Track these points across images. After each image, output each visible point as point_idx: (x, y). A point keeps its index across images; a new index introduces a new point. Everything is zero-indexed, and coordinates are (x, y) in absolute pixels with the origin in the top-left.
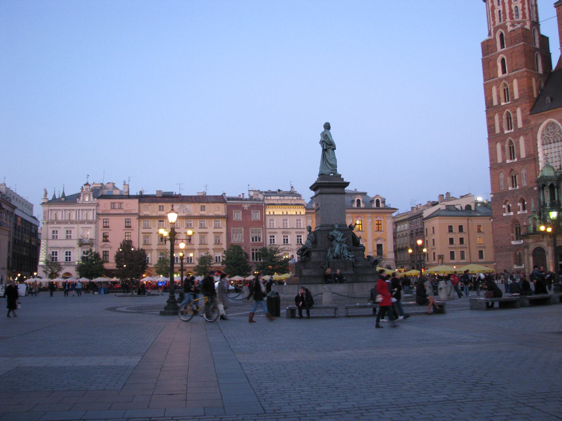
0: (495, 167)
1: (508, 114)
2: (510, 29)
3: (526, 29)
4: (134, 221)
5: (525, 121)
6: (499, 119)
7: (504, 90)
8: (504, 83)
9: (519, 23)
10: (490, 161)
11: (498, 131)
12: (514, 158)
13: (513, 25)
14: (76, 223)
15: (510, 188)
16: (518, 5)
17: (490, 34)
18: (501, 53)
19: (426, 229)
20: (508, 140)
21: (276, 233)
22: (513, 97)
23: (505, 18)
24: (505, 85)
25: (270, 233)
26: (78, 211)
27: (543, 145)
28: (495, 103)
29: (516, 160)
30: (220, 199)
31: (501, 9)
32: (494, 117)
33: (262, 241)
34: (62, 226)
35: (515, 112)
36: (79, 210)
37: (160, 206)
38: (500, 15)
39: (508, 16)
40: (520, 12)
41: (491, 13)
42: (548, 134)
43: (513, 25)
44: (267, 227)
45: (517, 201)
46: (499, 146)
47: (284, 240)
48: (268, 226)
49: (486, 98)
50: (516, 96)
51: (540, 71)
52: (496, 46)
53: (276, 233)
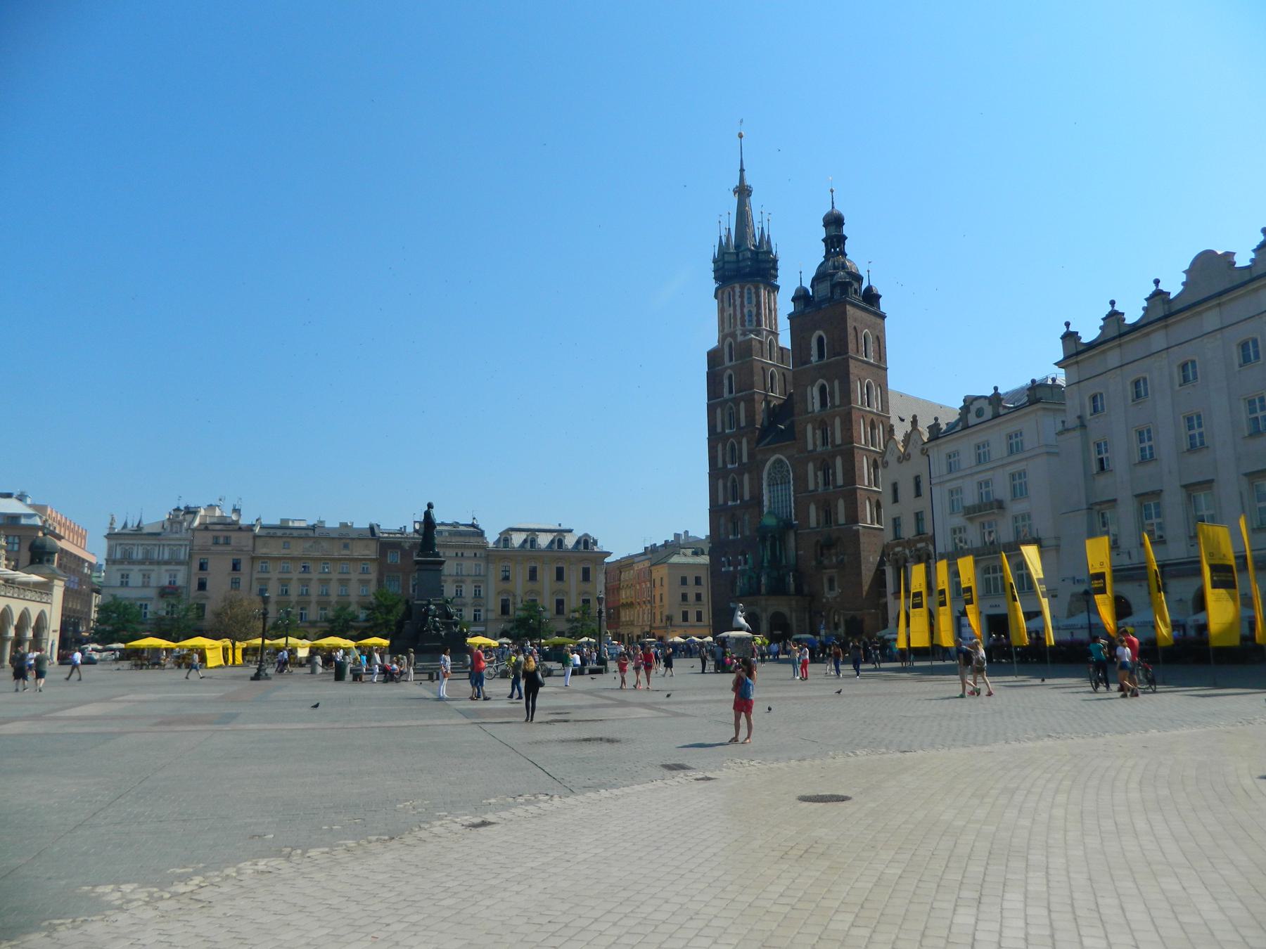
0: (716, 511)
1: (733, 446)
2: (740, 338)
4: (244, 567)
5: (751, 456)
6: (723, 450)
7: (730, 414)
9: (751, 332)
11: (720, 464)
13: (744, 334)
14: (159, 563)
16: (752, 309)
18: (729, 367)
19: (654, 580)
20: (730, 477)
23: (735, 325)
24: (731, 408)
26: (161, 548)
27: (769, 485)
28: (719, 429)
29: (739, 501)
31: (732, 312)
34: (136, 568)
35: (740, 443)
36: (164, 545)
37: (284, 543)
39: (739, 322)
40: (754, 319)
42: (774, 473)
46: (720, 483)
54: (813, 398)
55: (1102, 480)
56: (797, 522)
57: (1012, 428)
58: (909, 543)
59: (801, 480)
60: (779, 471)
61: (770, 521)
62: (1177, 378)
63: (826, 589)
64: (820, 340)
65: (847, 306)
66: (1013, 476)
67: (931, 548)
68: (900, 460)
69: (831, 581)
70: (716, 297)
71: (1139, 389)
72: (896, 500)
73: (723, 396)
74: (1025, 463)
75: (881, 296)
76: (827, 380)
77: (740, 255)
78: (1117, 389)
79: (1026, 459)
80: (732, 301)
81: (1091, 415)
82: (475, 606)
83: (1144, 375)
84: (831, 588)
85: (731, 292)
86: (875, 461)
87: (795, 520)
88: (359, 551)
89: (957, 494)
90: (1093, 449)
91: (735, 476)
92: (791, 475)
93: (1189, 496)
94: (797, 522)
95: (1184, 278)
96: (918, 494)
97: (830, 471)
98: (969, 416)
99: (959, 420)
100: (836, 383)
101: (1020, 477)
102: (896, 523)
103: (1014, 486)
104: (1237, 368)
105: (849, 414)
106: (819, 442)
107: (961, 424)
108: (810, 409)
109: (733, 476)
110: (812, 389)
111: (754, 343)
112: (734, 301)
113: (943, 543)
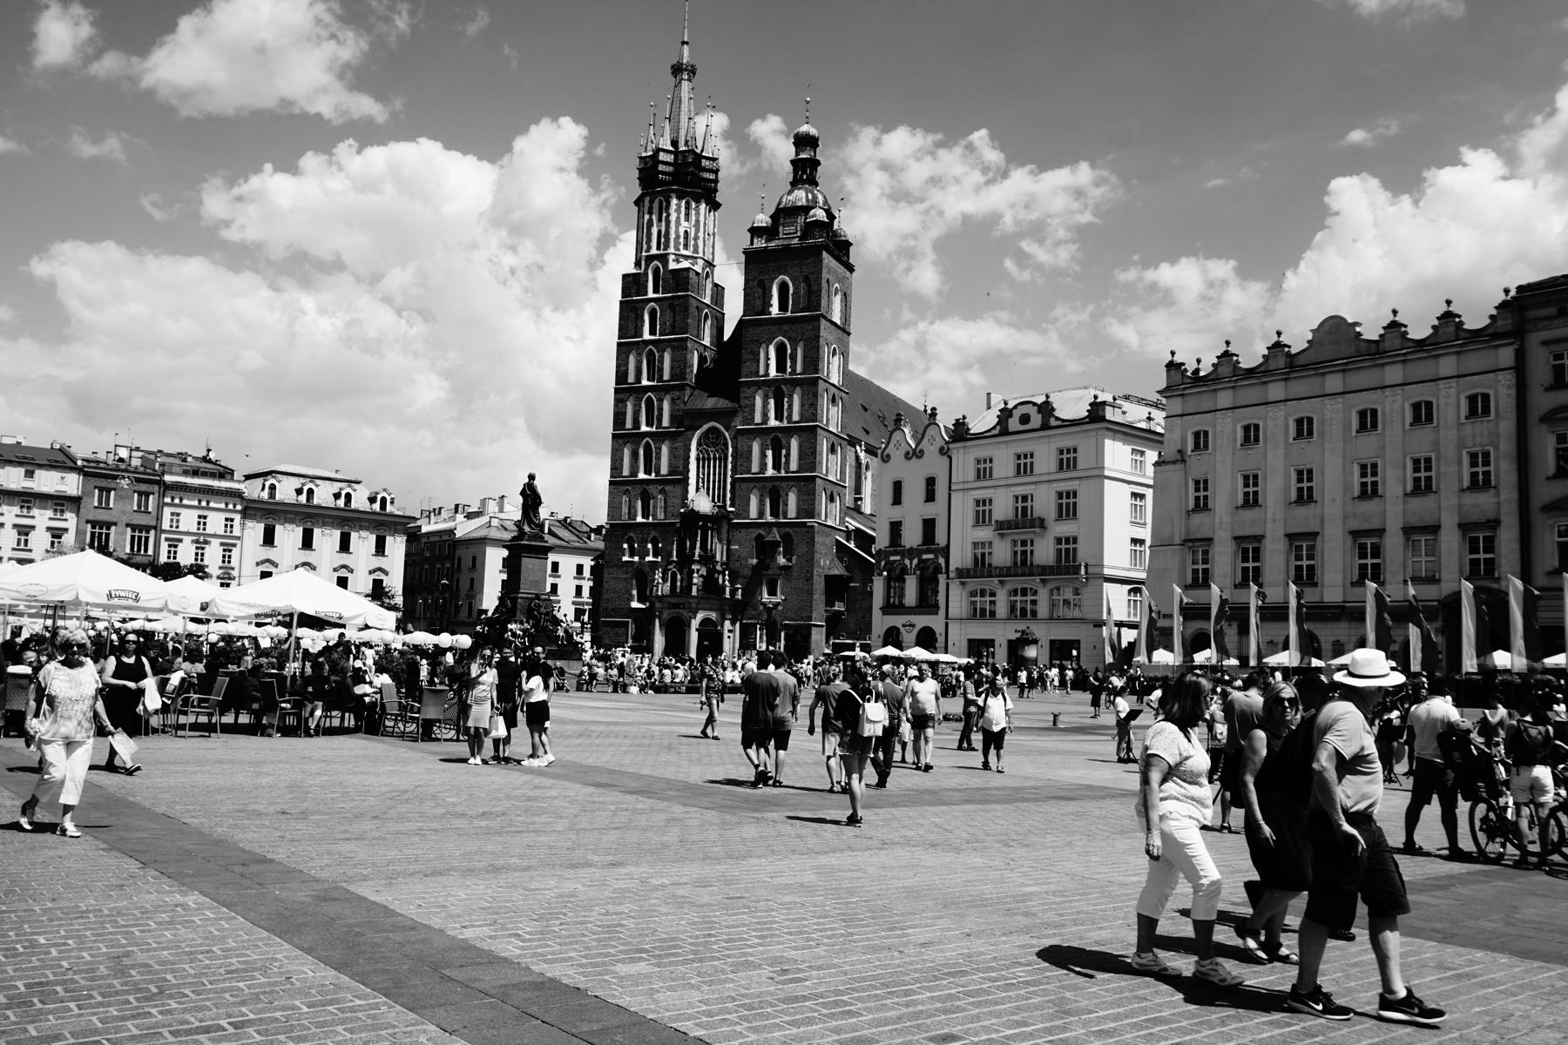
0: (618, 484)
1: (649, 401)
3: (697, 274)
6: (635, 405)
8: (651, 350)
9: (686, 257)
10: (612, 469)
12: (650, 474)
15: (639, 519)
17: (638, 264)
19: (459, 559)
21: (181, 541)
22: (660, 379)
23: (666, 247)
24: (651, 353)
25: (167, 539)
27: (698, 459)
29: (653, 474)
30: (61, 460)
33: (150, 552)
35: (661, 401)
43: (678, 262)
44: (163, 528)
45: (647, 542)
47: (197, 554)
48: (166, 525)
49: (618, 366)
50: (666, 377)
51: (707, 342)
52: (646, 287)
53: (181, 541)
54: (769, 359)
55: (1197, 519)
56: (733, 509)
57: (1066, 443)
58: (911, 553)
59: (742, 458)
60: (712, 443)
61: (702, 503)
62: (1292, 431)
63: (765, 595)
65: (825, 254)
66: (1060, 495)
67: (942, 561)
68: (907, 456)
70: (638, 202)
71: (1251, 435)
72: (897, 500)
73: (642, 336)
74: (1077, 482)
75: (851, 244)
77: (680, 157)
78: (1225, 430)
79: (1079, 478)
81: (1192, 451)
82: (223, 578)
83: (1256, 422)
84: (772, 592)
85: (664, 204)
86: (833, 443)
87: (731, 506)
88: (47, 481)
89: (984, 505)
90: (1191, 485)
91: (651, 442)
92: (730, 450)
93: (1291, 545)
94: (733, 509)
95: (1310, 336)
96: (930, 497)
97: (784, 452)
98: (1010, 420)
99: (997, 424)
101: (1068, 497)
102: (896, 528)
103: (1060, 505)
104: (1354, 433)
105: (815, 382)
106: (772, 414)
107: (998, 427)
108: (762, 372)
109: (647, 442)
111: (692, 275)
113: (960, 556)
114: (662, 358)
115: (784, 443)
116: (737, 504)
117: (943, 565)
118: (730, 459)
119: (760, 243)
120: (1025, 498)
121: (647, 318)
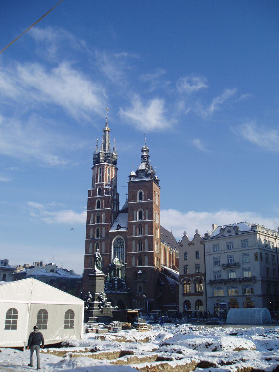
1: (98, 229)
7: (98, 216)
17: (93, 187)
20: (96, 242)
27: (114, 248)
32: (90, 230)
35: (102, 229)
38: (100, 179)
41: (96, 176)
46: (91, 245)
60: (118, 242)
63: (138, 291)
64: (141, 194)
69: (140, 288)
70: (92, 169)
76: (143, 209)
80: (102, 172)
86: (157, 242)
92: (125, 244)
96: (197, 257)
97: (143, 245)
100: (147, 211)
110: (136, 212)
112: (103, 172)
114: (101, 217)
115: (143, 242)
116: (127, 262)
117: (204, 279)
118: (125, 247)
119: (132, 180)
120: (231, 256)
121: (96, 203)
